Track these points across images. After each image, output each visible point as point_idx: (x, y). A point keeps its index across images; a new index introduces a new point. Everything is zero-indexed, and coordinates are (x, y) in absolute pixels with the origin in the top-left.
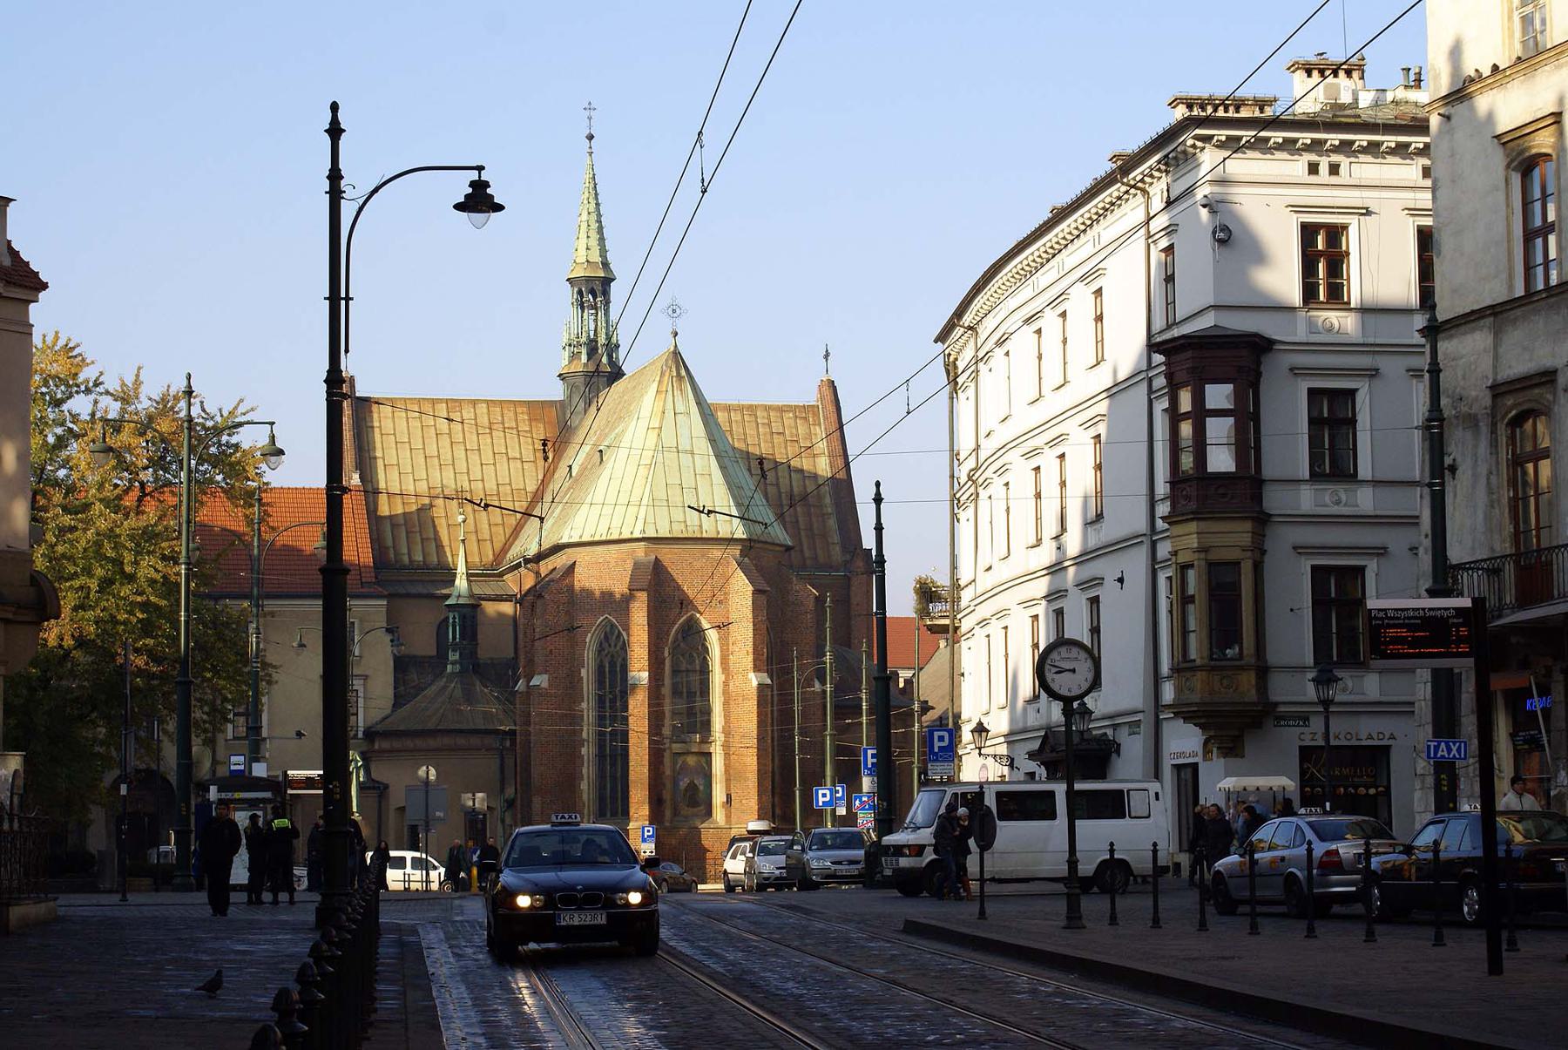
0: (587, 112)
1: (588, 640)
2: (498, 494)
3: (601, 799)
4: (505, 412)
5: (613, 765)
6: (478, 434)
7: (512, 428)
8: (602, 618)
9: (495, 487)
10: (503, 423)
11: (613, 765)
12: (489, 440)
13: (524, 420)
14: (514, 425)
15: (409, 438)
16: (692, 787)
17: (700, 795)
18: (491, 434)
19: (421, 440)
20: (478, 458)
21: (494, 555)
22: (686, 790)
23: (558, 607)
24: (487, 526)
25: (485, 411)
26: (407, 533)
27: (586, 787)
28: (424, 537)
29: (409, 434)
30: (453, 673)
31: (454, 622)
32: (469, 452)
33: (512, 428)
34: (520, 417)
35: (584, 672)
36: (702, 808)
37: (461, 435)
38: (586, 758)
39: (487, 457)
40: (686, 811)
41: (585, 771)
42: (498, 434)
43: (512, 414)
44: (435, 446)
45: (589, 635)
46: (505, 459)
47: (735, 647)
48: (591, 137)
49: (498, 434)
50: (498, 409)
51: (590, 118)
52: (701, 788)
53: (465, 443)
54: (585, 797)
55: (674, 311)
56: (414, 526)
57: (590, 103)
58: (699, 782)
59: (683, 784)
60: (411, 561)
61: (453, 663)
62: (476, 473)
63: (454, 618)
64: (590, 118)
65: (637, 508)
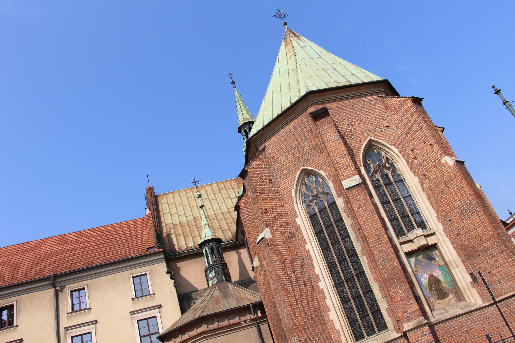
0: (230, 76)
1: (293, 195)
2: (229, 212)
3: (352, 322)
4: (226, 184)
5: (353, 287)
6: (214, 194)
7: (230, 188)
8: (298, 173)
9: (227, 210)
10: (225, 188)
11: (353, 287)
12: (220, 195)
13: (235, 185)
14: (230, 187)
15: (182, 203)
16: (434, 282)
17: (444, 285)
18: (220, 192)
19: (188, 202)
20: (216, 202)
21: (232, 234)
22: (430, 284)
23: (261, 178)
24: (226, 225)
25: (216, 186)
26: (184, 236)
27: (336, 316)
28: (193, 236)
29: (181, 201)
30: (213, 285)
31: (206, 254)
32: (211, 201)
33: (230, 188)
34: (233, 184)
35: (298, 221)
36: (451, 296)
37: (207, 196)
38: (325, 290)
39: (220, 200)
40: (439, 304)
41: (328, 301)
42: (224, 192)
43: (229, 184)
44: (195, 202)
45: (293, 191)
46: (229, 199)
47: (417, 152)
48: (233, 83)
49: (224, 192)
50: (222, 184)
51: (231, 78)
52: (441, 278)
53: (208, 198)
54: (337, 326)
55: (281, 15)
56: (188, 233)
57: (230, 73)
58: (438, 273)
59: (425, 280)
60: (187, 247)
61: (212, 279)
62: (216, 207)
63: (206, 251)
64: (231, 78)
65: (293, 57)
